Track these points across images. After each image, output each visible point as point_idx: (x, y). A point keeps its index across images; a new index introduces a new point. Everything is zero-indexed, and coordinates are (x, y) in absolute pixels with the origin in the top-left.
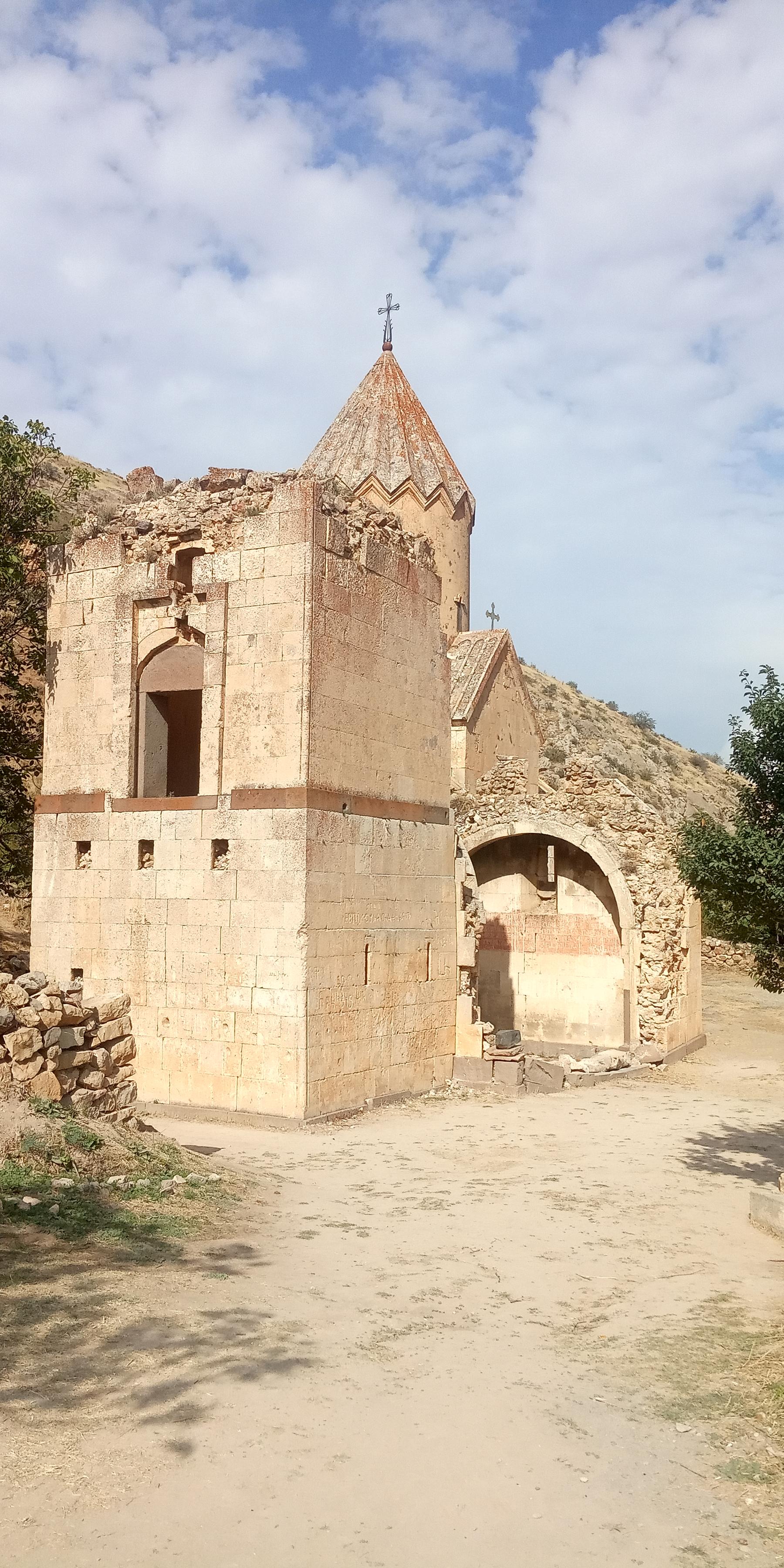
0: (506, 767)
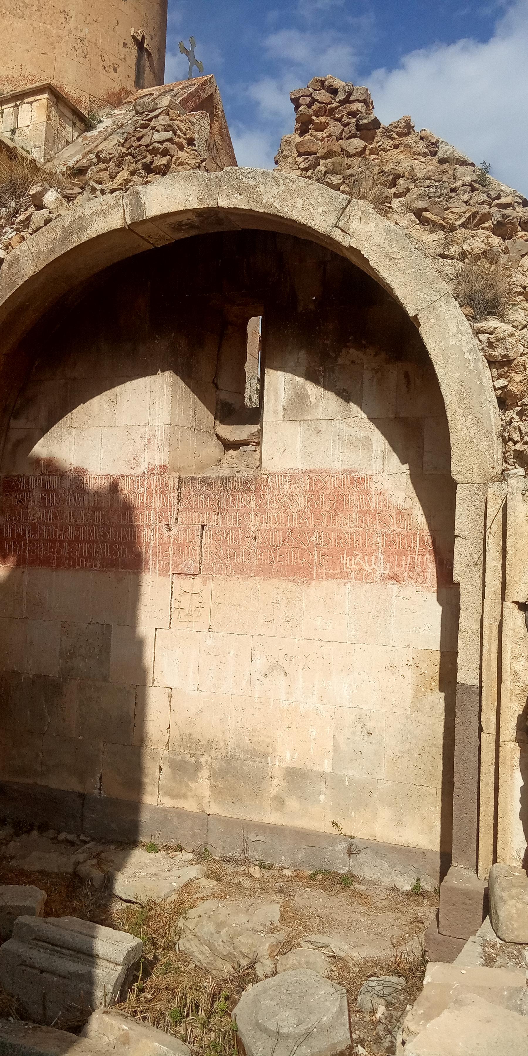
0: (152, 124)
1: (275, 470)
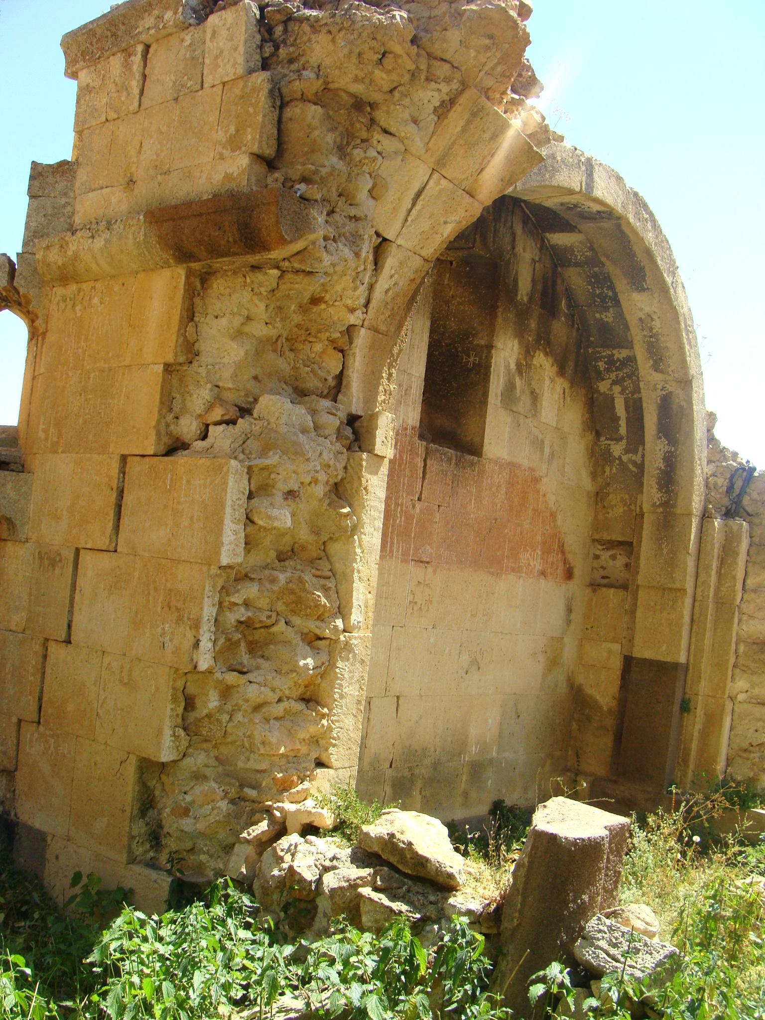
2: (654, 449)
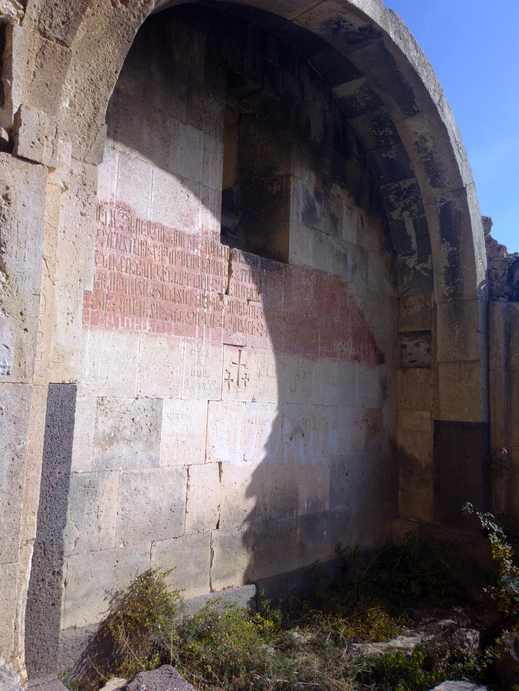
1: (297, 264)
2: (440, 252)
